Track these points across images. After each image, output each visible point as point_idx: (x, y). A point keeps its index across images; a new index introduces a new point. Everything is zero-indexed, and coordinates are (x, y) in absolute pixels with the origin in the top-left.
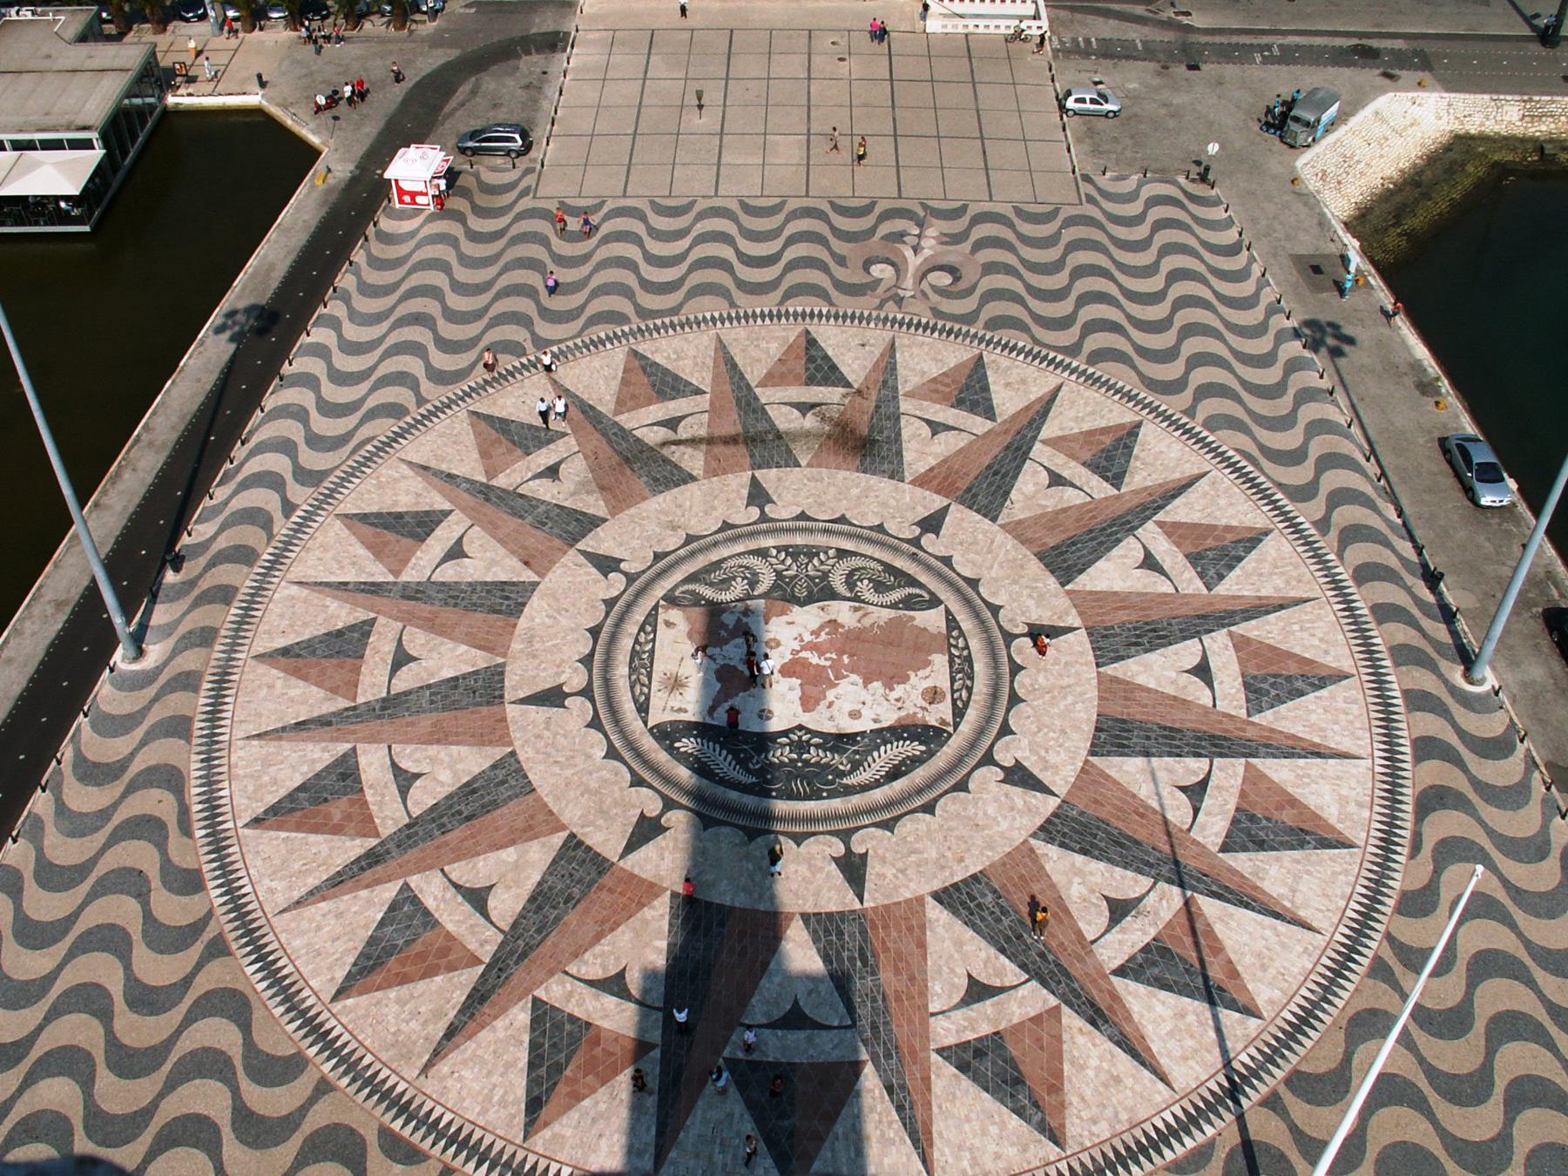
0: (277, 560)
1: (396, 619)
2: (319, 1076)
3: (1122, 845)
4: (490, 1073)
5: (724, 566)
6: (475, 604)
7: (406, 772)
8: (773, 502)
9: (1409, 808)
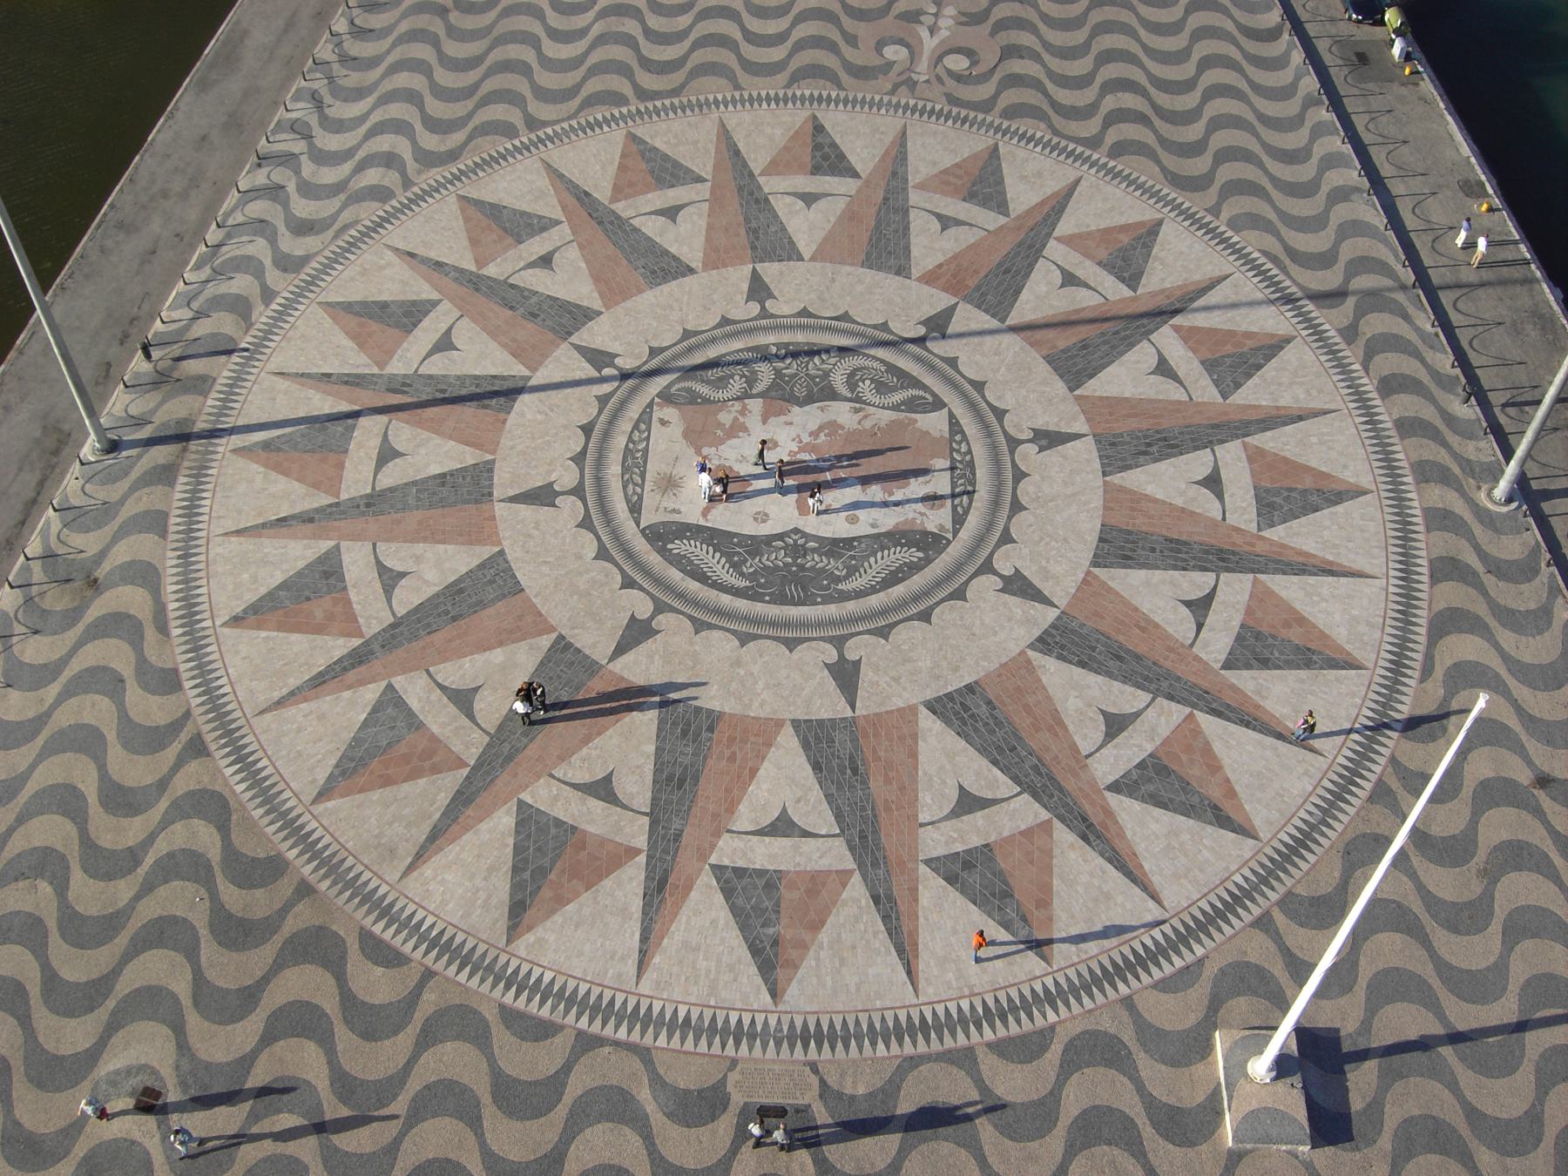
0: (258, 347)
7: (391, 570)
9: (1423, 631)
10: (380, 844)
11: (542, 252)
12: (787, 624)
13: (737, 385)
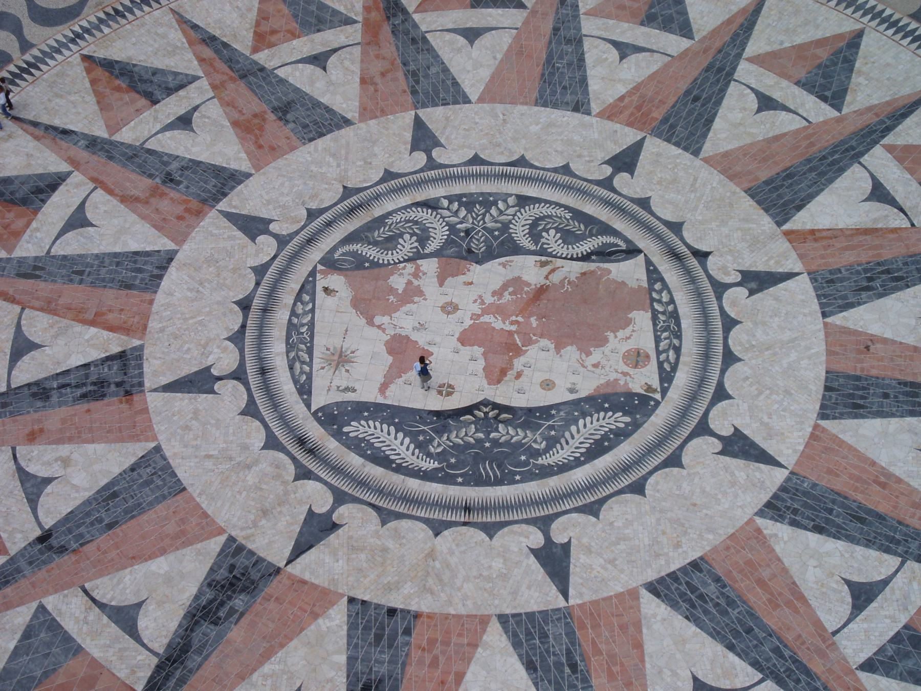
3: (861, 520)
5: (389, 221)
6: (103, 280)
8: (442, 146)
11: (182, 112)
13: (408, 245)
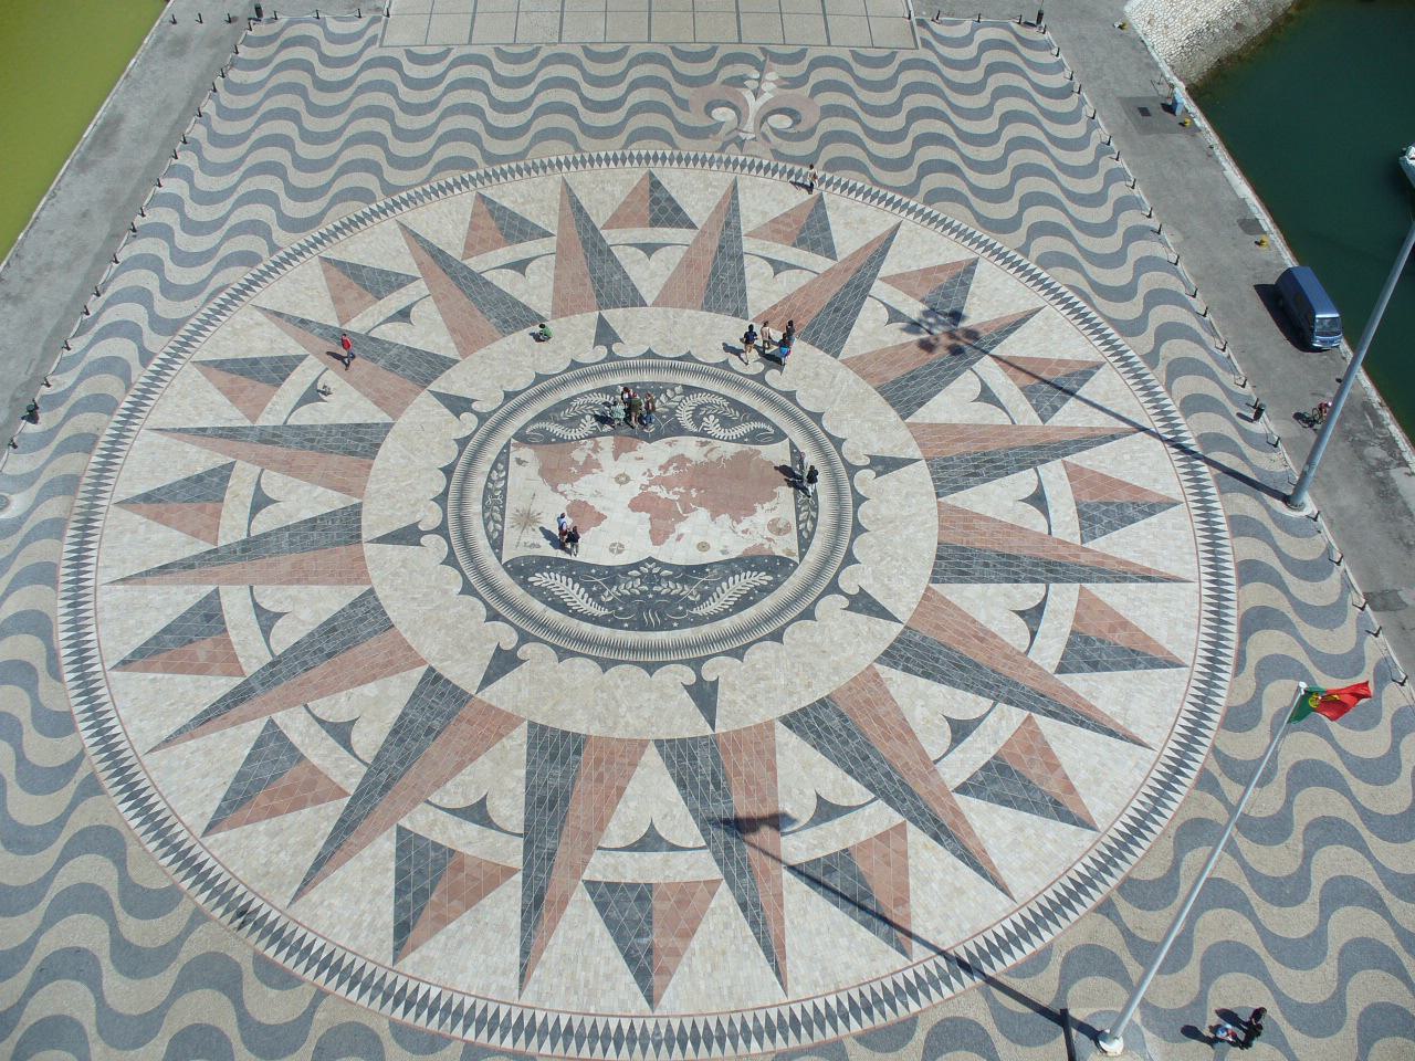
0: (136, 408)
1: (255, 462)
2: (192, 907)
3: (962, 668)
4: (358, 902)
6: (330, 447)
9: (1234, 628)
10: (268, 873)
12: (647, 649)
